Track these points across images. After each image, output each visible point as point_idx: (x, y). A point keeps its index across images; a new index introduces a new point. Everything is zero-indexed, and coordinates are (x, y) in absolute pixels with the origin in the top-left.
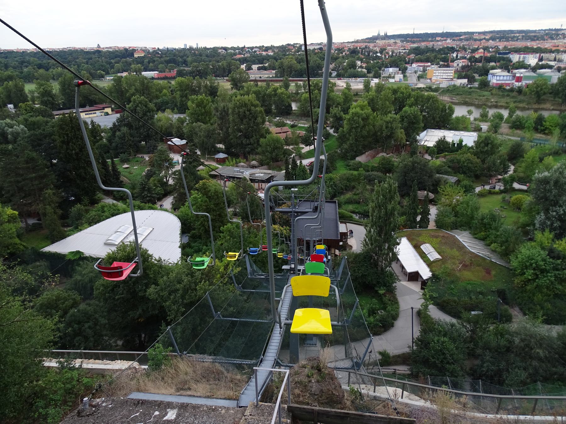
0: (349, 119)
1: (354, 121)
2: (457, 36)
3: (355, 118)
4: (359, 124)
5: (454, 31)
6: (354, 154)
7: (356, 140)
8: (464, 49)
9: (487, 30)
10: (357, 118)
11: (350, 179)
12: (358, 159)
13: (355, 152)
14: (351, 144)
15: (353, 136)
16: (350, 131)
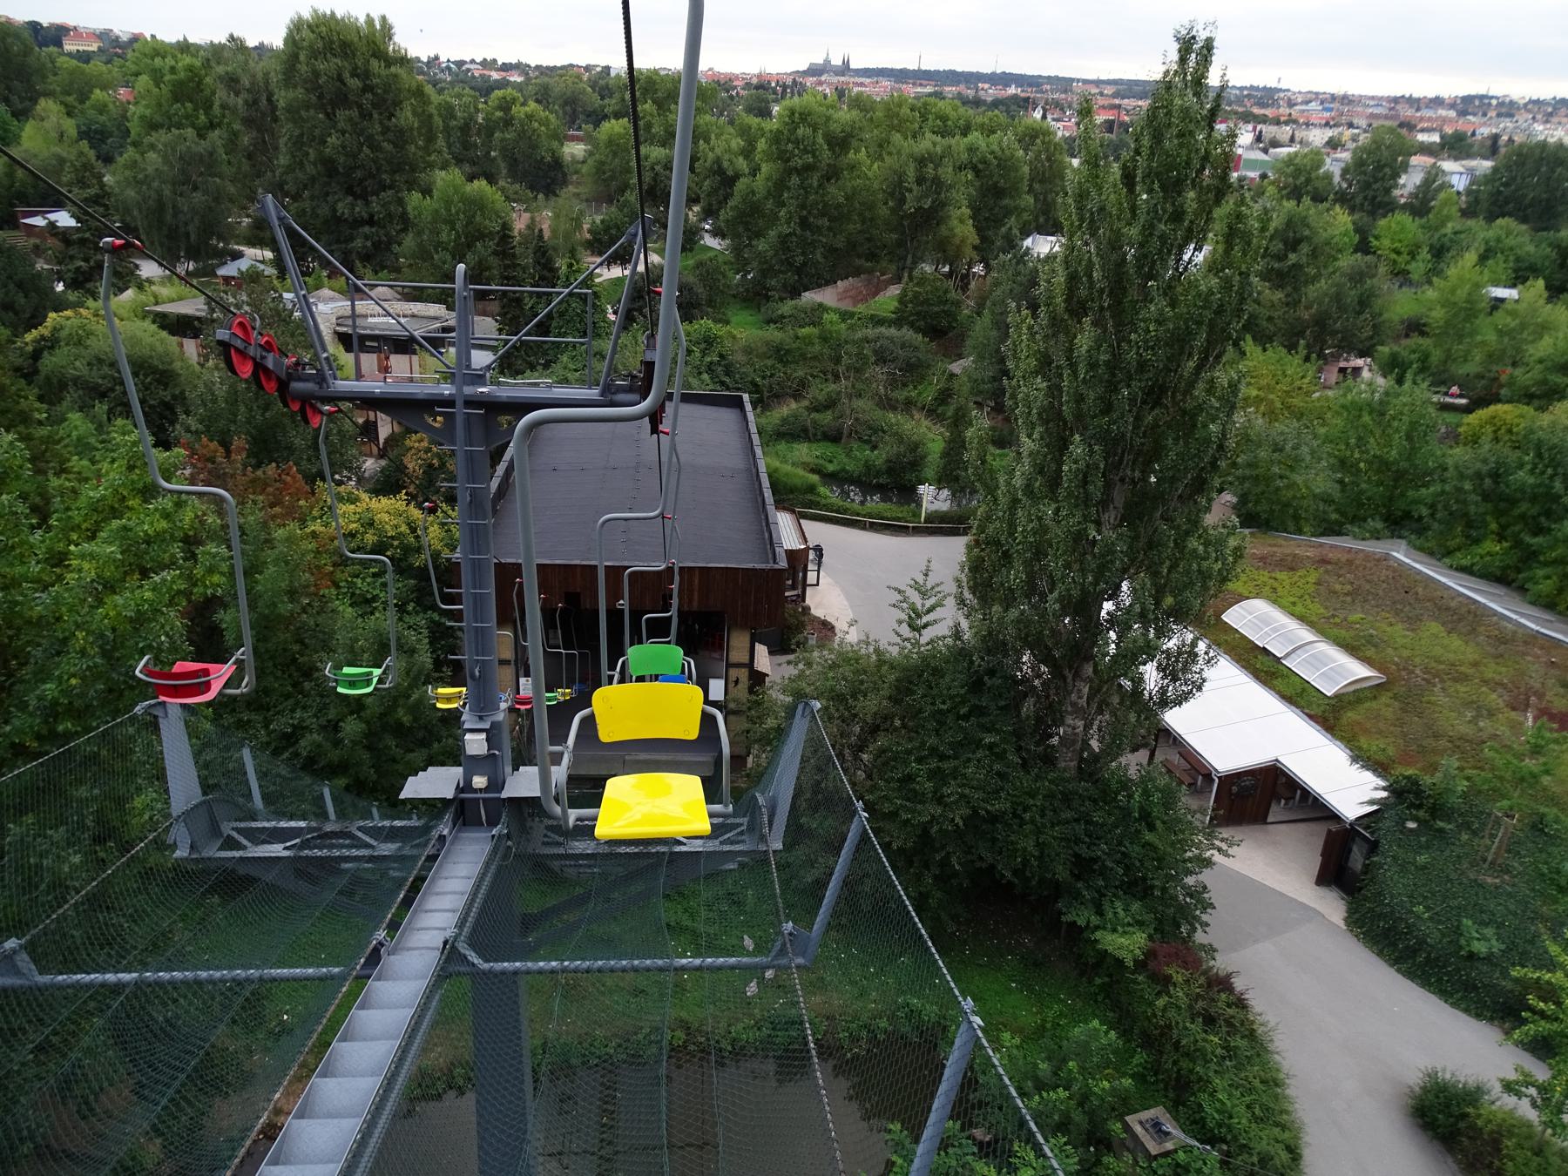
0: (776, 138)
1: (797, 142)
2: (1030, 85)
3: (800, 132)
4: (814, 156)
5: (1022, 72)
6: (792, 277)
7: (804, 223)
8: (1058, 105)
9: (1104, 77)
10: (809, 131)
11: (788, 352)
12: (810, 297)
13: (799, 271)
14: (784, 240)
15: (792, 205)
16: (780, 185)
